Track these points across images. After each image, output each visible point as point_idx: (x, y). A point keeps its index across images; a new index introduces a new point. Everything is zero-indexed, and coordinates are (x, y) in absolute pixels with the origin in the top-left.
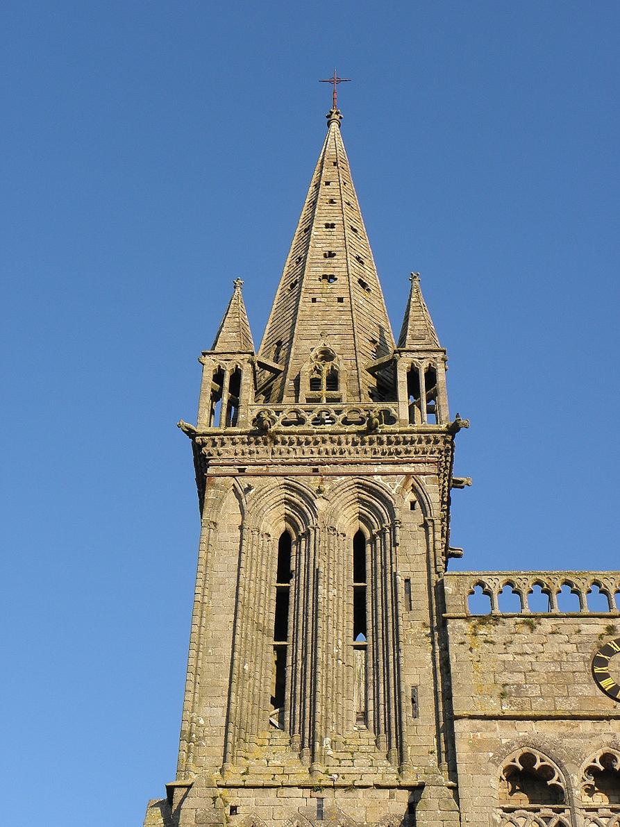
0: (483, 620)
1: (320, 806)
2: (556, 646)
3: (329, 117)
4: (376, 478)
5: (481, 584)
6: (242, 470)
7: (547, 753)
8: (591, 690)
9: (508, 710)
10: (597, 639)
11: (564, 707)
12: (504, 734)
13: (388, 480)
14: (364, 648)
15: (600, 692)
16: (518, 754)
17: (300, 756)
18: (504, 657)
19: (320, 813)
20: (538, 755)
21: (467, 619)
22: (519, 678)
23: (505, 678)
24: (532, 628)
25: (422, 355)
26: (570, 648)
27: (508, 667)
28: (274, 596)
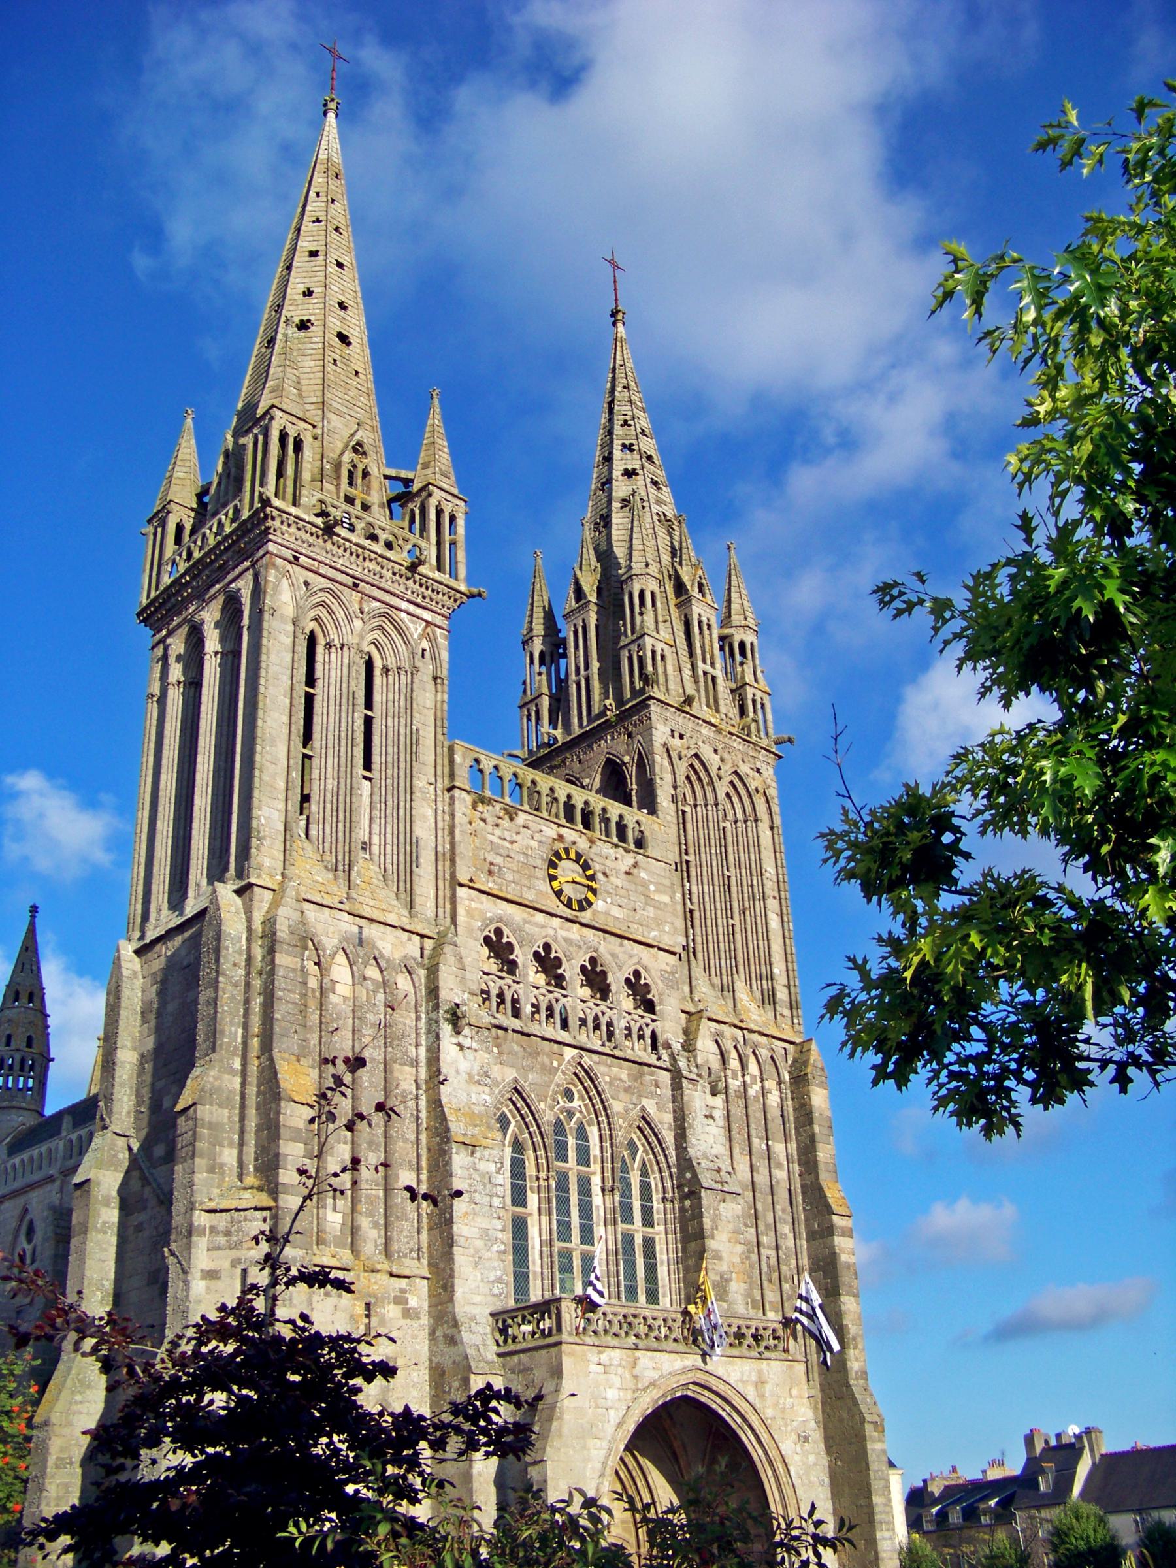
0: (483, 800)
1: (360, 933)
2: (524, 840)
3: (325, 105)
4: (403, 615)
5: (477, 761)
6: (297, 558)
7: (514, 932)
8: (544, 886)
9: (489, 886)
10: (550, 841)
11: (529, 897)
13: (412, 622)
14: (370, 779)
15: (550, 891)
16: (492, 928)
17: (336, 878)
18: (491, 837)
19: (360, 939)
20: (506, 931)
21: (468, 792)
22: (499, 860)
23: (491, 857)
24: (511, 819)
25: (449, 497)
26: (534, 844)
27: (494, 848)
28: (303, 701)
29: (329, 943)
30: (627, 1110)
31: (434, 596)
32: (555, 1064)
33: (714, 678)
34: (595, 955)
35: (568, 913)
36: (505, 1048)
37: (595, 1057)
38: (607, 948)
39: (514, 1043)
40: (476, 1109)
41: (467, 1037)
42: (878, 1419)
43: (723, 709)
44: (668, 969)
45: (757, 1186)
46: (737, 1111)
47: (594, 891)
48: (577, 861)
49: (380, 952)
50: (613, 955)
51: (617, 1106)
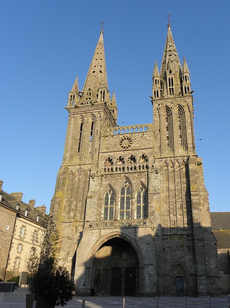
0: (106, 137)
8: (119, 147)
11: (115, 150)
12: (106, 155)
18: (108, 142)
25: (103, 89)
29: (74, 171)
30: (136, 182)
31: (99, 107)
32: (119, 178)
33: (173, 89)
34: (131, 155)
35: (124, 149)
36: (107, 178)
37: (129, 174)
38: (133, 153)
39: (109, 177)
40: (96, 191)
41: (95, 179)
42: (199, 238)
43: (174, 94)
44: (151, 152)
45: (176, 190)
46: (171, 175)
47: (131, 144)
48: (127, 139)
49: (84, 169)
50: (135, 154)
51: (134, 182)
